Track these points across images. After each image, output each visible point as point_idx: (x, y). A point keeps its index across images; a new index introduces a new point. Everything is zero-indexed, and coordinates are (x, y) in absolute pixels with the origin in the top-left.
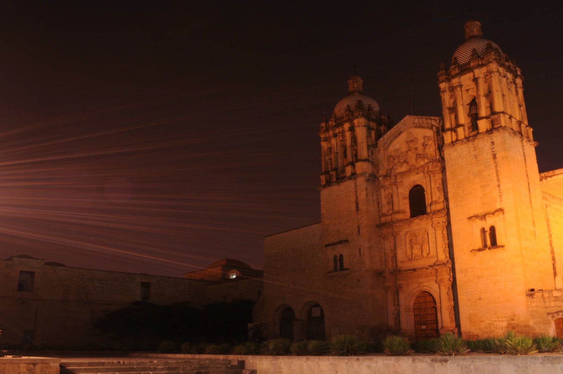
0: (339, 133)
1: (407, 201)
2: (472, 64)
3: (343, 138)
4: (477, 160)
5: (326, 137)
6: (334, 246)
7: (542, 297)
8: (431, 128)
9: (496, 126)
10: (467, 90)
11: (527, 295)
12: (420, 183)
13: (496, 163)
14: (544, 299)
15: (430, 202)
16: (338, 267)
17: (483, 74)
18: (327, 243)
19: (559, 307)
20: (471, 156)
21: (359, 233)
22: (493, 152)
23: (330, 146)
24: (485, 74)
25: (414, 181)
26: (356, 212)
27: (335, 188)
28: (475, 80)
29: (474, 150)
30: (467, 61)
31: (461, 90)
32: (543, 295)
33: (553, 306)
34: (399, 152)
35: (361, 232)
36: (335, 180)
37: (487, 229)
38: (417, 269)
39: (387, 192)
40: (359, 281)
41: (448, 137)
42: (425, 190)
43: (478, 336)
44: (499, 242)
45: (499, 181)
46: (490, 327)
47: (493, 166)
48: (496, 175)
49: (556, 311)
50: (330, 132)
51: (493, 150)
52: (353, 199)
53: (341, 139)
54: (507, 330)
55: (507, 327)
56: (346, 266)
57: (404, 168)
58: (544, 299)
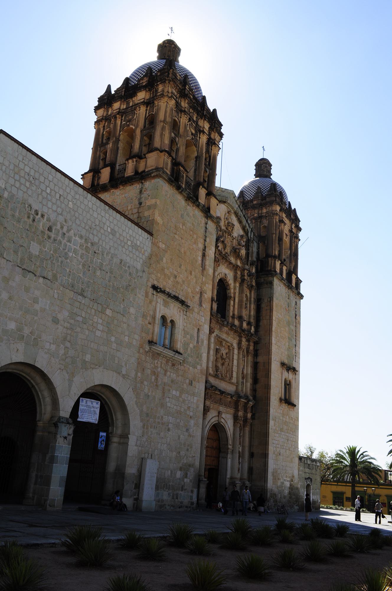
3: (195, 134)
6: (169, 300)
12: (230, 283)
18: (156, 283)
23: (177, 119)
27: (180, 200)
32: (304, 461)
35: (204, 306)
38: (225, 392)
40: (191, 384)
42: (232, 295)
45: (296, 341)
46: (282, 487)
47: (295, 324)
50: (183, 100)
52: (201, 246)
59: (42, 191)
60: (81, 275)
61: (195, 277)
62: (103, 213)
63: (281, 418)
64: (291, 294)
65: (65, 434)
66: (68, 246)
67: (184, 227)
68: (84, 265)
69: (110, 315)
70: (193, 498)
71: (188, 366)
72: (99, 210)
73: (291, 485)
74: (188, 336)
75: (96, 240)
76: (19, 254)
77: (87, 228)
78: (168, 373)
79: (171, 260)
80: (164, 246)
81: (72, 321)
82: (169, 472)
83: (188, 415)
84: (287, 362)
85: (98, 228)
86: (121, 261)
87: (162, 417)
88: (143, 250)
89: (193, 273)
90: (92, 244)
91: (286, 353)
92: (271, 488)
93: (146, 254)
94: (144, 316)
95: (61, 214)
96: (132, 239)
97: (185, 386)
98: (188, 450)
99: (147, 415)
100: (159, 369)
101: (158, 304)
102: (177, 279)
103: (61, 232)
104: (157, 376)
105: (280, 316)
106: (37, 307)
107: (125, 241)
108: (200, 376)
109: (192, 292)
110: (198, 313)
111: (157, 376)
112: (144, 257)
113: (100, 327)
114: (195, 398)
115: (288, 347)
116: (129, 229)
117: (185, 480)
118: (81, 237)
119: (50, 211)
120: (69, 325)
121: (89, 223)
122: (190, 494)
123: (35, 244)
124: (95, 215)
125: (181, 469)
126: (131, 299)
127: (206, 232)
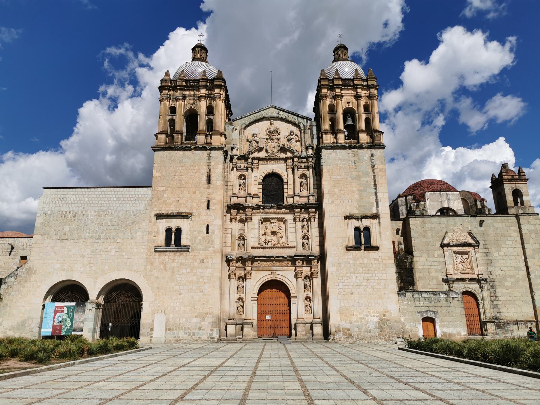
0: (191, 95)
1: (261, 186)
2: (356, 82)
3: (194, 102)
4: (356, 166)
5: (169, 93)
7: (413, 297)
8: (297, 125)
9: (377, 142)
10: (348, 103)
11: (398, 294)
13: (374, 173)
14: (414, 299)
15: (291, 192)
16: (173, 242)
17: (364, 94)
18: (158, 212)
19: (428, 307)
20: (350, 160)
21: (208, 208)
22: (372, 162)
24: (367, 94)
25: (273, 170)
26: (207, 185)
28: (358, 97)
29: (354, 156)
30: (349, 77)
31: (342, 101)
33: (422, 305)
34: (258, 136)
36: (179, 143)
37: (362, 229)
39: (239, 173)
41: (328, 139)
42: (285, 181)
43: (348, 330)
44: (374, 243)
45: (376, 189)
46: (362, 321)
48: (373, 183)
49: (425, 310)
51: (373, 161)
52: (204, 171)
53: (191, 101)
54: (379, 325)
55: (379, 322)
56: (184, 242)
57: (262, 155)
58: (414, 299)
59: (68, 201)
60: (97, 230)
61: (200, 193)
62: (110, 193)
63: (351, 262)
64: (360, 151)
65: (91, 308)
66: (87, 219)
67: (184, 168)
68: (98, 224)
69: (121, 242)
70: (213, 334)
71: (198, 251)
72: (106, 193)
73: (381, 320)
74: (196, 233)
75: (106, 208)
76: (58, 234)
77: (98, 205)
78: (177, 261)
79: (172, 193)
80: (164, 188)
81: (93, 253)
82: (184, 320)
83: (202, 282)
84: (358, 212)
85: (107, 202)
86: (126, 211)
87: (173, 288)
88: (144, 198)
89: (197, 192)
90: (103, 211)
91: (356, 204)
92: (338, 323)
93: (148, 199)
94: (149, 234)
95: (81, 206)
96: (134, 196)
97: (196, 264)
98: (203, 304)
99: (158, 288)
100: (167, 260)
101: (161, 223)
102: (179, 202)
103: (81, 215)
104: (166, 265)
105: (338, 177)
106: (70, 253)
107: (129, 199)
108: (213, 255)
109: (197, 204)
110: (207, 215)
111: (166, 265)
112: (146, 202)
113: (114, 250)
114: (209, 271)
115: (359, 199)
116: (131, 191)
117: (203, 323)
118: (95, 211)
119: (74, 208)
120: (91, 256)
121: (100, 202)
122: (209, 332)
123: (67, 226)
124: (104, 196)
125: (196, 317)
126: (137, 228)
127: (209, 159)
